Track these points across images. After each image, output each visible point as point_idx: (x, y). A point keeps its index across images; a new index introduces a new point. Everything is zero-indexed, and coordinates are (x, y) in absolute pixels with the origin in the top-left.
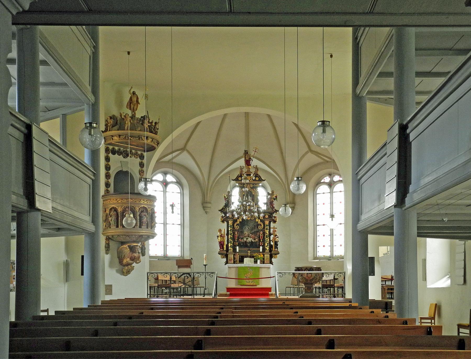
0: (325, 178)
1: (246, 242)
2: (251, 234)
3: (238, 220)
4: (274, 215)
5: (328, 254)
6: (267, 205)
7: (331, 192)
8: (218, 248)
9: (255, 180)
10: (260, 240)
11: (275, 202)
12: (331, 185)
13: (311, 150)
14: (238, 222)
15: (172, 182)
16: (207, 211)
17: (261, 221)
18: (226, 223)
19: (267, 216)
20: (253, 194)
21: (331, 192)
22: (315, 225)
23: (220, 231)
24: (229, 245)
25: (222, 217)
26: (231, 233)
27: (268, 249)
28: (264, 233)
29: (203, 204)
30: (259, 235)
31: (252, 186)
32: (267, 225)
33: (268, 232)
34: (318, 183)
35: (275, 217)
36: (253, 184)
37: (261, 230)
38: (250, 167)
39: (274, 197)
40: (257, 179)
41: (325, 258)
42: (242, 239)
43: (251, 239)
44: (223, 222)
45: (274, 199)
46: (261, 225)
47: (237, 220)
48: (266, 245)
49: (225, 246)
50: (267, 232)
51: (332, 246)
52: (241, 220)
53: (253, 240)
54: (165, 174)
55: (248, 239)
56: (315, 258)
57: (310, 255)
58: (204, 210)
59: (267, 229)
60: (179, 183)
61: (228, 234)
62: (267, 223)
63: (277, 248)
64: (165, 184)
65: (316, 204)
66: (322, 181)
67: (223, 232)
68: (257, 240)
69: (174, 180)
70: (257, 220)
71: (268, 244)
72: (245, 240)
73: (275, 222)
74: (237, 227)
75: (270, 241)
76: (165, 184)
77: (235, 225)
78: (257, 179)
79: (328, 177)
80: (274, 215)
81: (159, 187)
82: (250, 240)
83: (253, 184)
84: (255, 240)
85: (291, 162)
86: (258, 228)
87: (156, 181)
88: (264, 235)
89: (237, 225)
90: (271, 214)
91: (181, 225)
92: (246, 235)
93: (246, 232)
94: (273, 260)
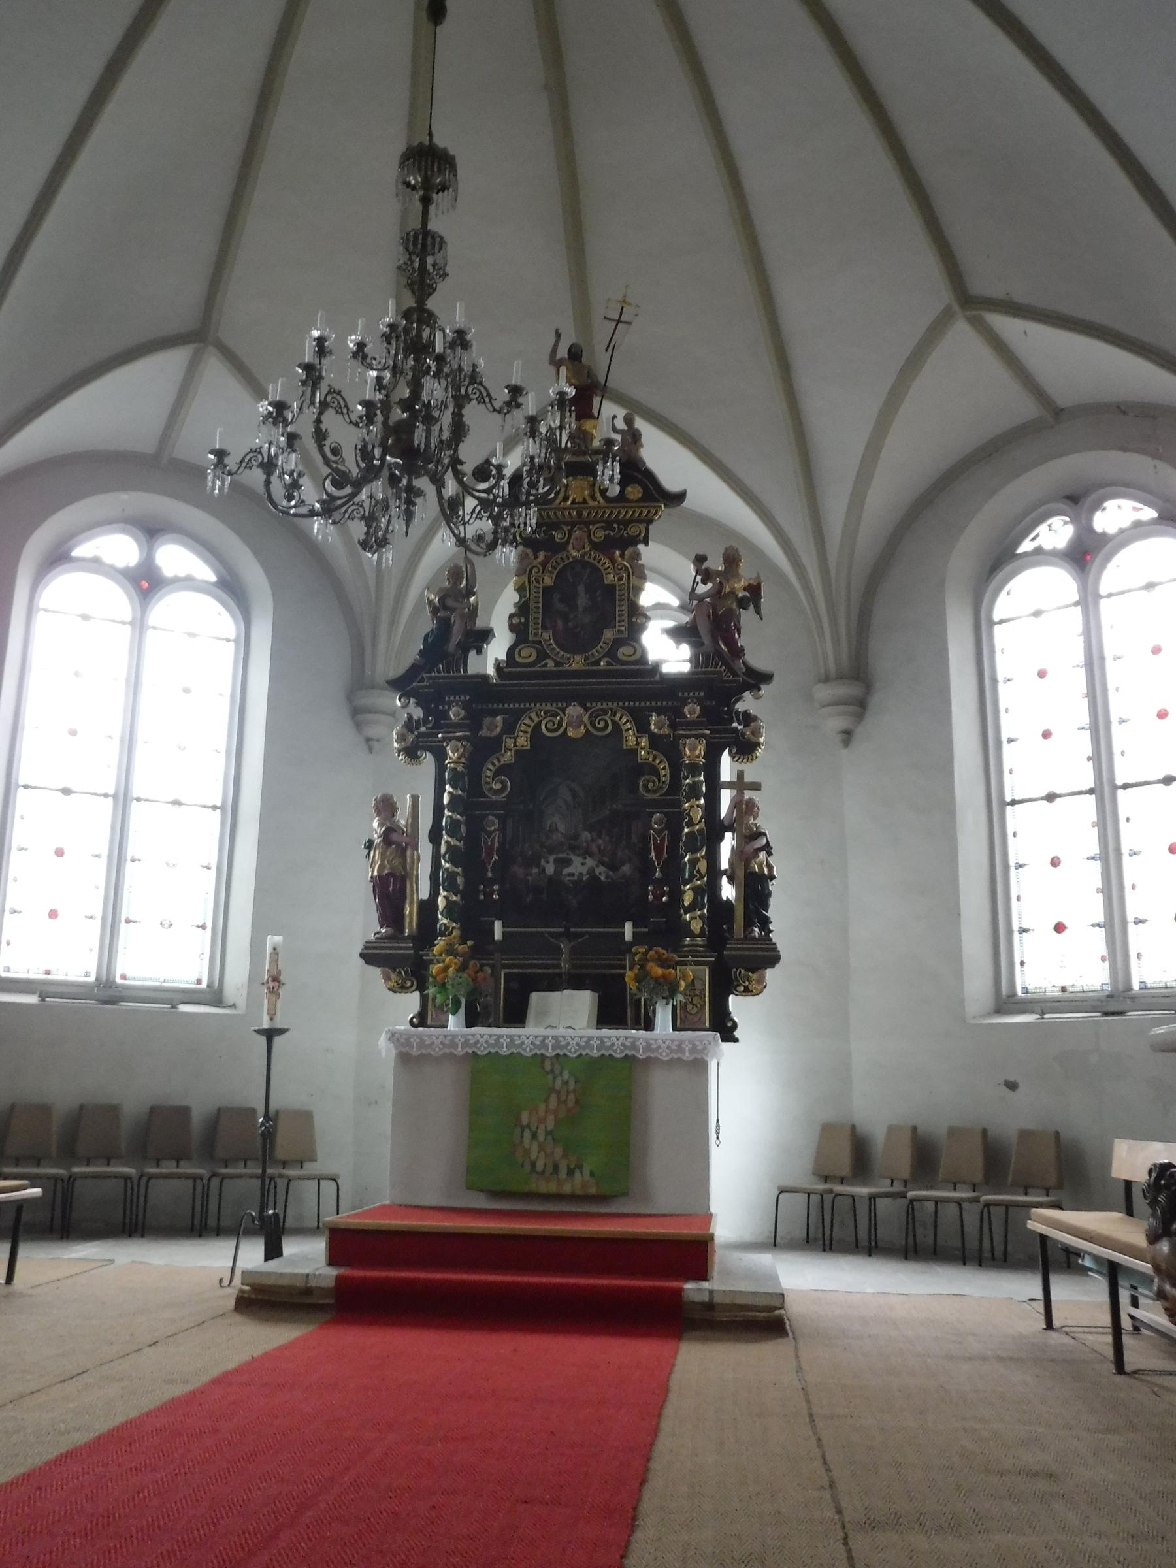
0: (1042, 529)
1: (554, 883)
2: (590, 828)
3: (510, 742)
4: (740, 707)
5: (1093, 976)
6: (696, 644)
7: (1089, 600)
8: (365, 923)
9: (621, 497)
10: (645, 870)
11: (747, 617)
12: (1085, 555)
13: (969, 302)
14: (508, 757)
15: (188, 583)
16: (372, 732)
17: (656, 742)
18: (428, 760)
19: (692, 711)
20: (610, 578)
21: (1089, 600)
22: (996, 805)
23: (386, 807)
24: (441, 903)
25: (410, 725)
26: (454, 824)
27: (696, 926)
28: (676, 819)
29: (350, 698)
30: (645, 838)
31: (599, 535)
32: (694, 769)
33: (698, 814)
34: (1000, 560)
35: (748, 719)
36: (608, 525)
37: (657, 805)
38: (588, 425)
39: (739, 587)
40: (634, 492)
41: (1068, 1001)
42: (534, 861)
43: (590, 863)
44: (411, 753)
45: (743, 603)
46: (655, 771)
47: (498, 741)
48: (688, 899)
49: (410, 911)
50: (695, 809)
51: (1115, 926)
52: (523, 741)
53: (602, 872)
54: (151, 531)
55: (567, 862)
56: (1007, 1002)
57: (977, 987)
58: (358, 726)
59: (694, 792)
60: (231, 588)
61: (435, 837)
62: (694, 750)
63: (765, 923)
64: (146, 583)
65: (995, 681)
66: (1026, 546)
67: (402, 820)
68: (626, 869)
69: (206, 573)
70: (631, 739)
71: (696, 890)
72: (550, 869)
73: (745, 749)
74: (495, 786)
75: (714, 872)
76: (146, 583)
77: (488, 771)
78: (634, 492)
79: (1057, 521)
80: (740, 707)
81: (117, 600)
82: (579, 867)
83: (608, 525)
84: (613, 867)
85: (840, 420)
86: (634, 789)
87: (95, 565)
88: (676, 835)
89: (501, 770)
90: (719, 697)
91: (223, 808)
92: (557, 837)
93: (558, 823)
94: (735, 1004)
